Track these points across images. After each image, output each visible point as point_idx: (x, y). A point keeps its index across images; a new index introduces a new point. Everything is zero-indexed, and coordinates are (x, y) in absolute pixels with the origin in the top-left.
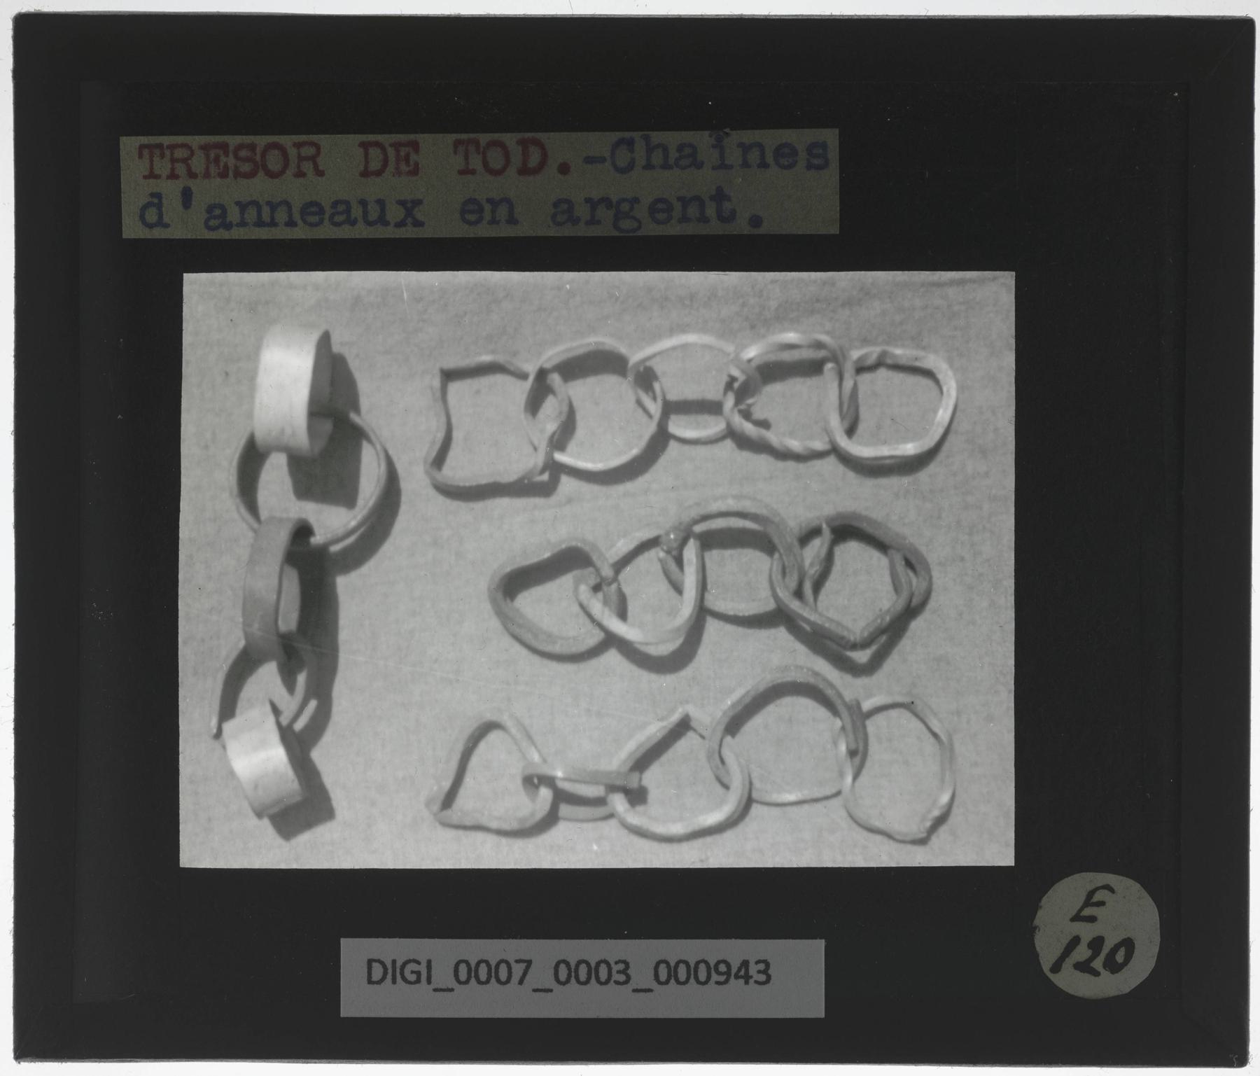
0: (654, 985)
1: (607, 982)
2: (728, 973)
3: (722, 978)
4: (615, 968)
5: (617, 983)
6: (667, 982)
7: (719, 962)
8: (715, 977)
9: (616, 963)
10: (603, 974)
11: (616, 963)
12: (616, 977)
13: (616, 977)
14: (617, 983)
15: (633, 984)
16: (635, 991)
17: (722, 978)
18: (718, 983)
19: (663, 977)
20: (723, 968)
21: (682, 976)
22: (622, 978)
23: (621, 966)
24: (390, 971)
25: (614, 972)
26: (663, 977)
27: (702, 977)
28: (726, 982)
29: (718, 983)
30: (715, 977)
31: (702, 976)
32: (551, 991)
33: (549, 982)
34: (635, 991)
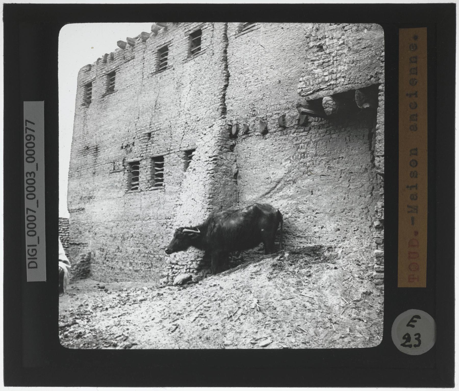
0: (35, 163)
1: (34, 180)
2: (30, 135)
3: (32, 138)
4: (29, 177)
5: (34, 177)
6: (34, 158)
7: (27, 139)
8: (32, 141)
9: (27, 177)
10: (32, 182)
11: (27, 177)
12: (32, 177)
13: (32, 177)
14: (34, 177)
15: (35, 170)
16: (37, 170)
17: (32, 138)
18: (34, 140)
19: (32, 160)
20: (28, 138)
21: (32, 153)
22: (33, 175)
23: (28, 175)
24: (32, 257)
25: (30, 178)
26: (32, 160)
27: (31, 145)
28: (33, 136)
29: (34, 140)
30: (32, 141)
31: (31, 145)
32: (38, 201)
33: (35, 201)
34: (37, 170)
